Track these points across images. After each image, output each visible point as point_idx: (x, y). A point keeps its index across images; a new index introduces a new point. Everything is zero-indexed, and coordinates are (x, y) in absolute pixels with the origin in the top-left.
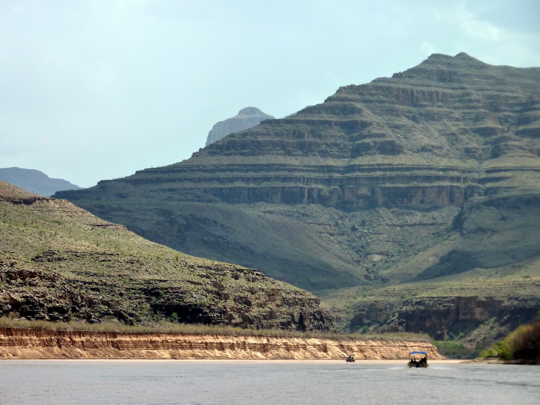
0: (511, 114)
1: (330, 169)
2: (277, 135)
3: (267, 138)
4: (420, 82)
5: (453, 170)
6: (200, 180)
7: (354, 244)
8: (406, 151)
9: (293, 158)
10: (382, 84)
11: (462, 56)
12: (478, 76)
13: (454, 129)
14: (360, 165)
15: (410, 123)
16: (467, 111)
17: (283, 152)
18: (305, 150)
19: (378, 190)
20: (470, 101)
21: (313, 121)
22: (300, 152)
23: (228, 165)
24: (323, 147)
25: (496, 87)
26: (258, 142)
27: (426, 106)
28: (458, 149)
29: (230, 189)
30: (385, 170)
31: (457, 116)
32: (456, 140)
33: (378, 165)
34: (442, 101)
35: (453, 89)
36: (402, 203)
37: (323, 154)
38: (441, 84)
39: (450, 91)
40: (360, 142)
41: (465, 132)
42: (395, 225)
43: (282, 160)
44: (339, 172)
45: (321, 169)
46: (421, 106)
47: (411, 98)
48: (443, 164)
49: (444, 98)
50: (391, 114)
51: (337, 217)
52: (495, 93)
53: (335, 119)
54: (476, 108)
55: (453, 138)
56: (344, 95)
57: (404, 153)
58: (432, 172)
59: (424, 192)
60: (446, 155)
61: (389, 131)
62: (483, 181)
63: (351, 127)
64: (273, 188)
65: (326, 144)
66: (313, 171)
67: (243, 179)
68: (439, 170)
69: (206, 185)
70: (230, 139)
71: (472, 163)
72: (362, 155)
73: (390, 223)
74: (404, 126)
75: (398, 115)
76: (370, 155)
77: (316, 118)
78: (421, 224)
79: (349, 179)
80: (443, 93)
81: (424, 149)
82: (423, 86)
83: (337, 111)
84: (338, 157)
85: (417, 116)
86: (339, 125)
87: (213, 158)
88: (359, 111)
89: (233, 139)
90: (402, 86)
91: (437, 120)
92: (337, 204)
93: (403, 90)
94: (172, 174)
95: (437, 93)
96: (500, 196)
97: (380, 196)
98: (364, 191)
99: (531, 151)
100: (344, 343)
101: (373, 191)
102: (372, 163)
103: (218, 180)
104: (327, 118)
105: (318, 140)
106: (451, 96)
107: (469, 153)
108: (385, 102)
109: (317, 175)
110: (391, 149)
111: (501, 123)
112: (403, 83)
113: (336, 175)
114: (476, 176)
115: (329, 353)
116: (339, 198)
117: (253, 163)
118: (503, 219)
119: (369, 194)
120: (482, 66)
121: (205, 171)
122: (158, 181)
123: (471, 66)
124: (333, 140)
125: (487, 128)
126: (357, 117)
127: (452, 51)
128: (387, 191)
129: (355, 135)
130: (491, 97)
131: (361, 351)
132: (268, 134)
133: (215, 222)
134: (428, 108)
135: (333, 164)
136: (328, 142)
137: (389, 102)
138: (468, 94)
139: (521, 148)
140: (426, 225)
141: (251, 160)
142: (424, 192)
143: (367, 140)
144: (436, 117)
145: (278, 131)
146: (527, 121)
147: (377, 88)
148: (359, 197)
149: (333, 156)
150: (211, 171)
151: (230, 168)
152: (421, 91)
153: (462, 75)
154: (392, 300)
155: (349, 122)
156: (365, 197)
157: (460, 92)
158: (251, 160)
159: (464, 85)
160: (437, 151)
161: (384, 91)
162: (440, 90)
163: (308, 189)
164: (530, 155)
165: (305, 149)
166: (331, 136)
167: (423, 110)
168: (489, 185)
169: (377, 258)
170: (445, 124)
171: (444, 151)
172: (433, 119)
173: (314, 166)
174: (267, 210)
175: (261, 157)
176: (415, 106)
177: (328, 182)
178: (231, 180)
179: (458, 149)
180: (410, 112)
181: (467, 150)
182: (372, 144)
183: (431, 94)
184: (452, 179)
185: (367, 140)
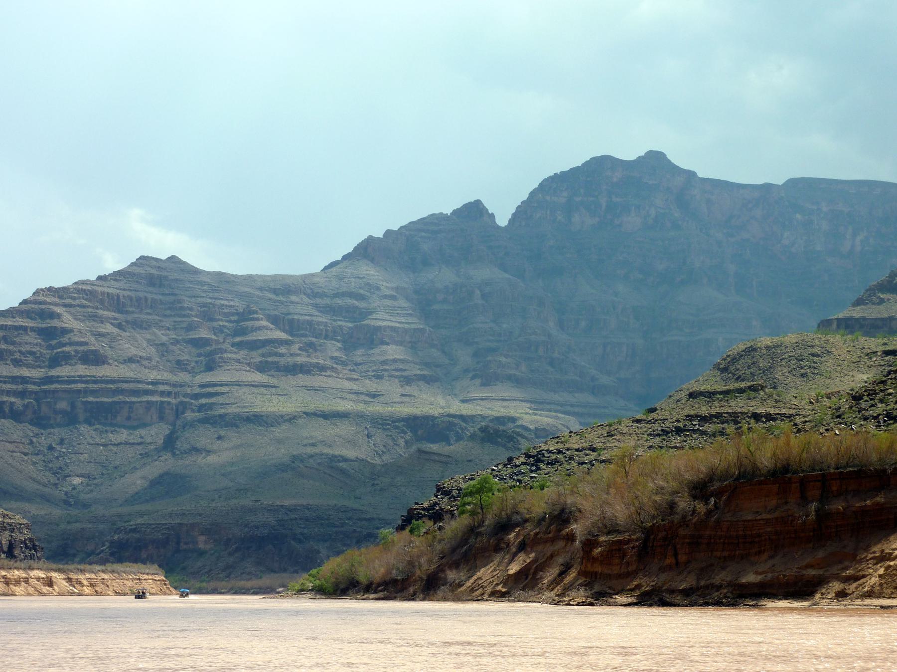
0: (226, 324)
1: (24, 380)
4: (127, 286)
5: (163, 384)
7: (51, 465)
8: (111, 361)
11: (173, 259)
12: (190, 282)
13: (164, 339)
14: (59, 377)
15: (115, 331)
20: (182, 308)
24: (17, 356)
25: (211, 295)
27: (133, 312)
28: (169, 361)
30: (87, 382)
33: (79, 376)
34: (151, 307)
35: (163, 294)
36: (106, 419)
37: (17, 363)
38: (151, 289)
39: (161, 297)
40: (59, 350)
42: (98, 444)
44: (34, 383)
45: (14, 380)
46: (127, 312)
47: (116, 303)
50: (94, 320)
51: (32, 434)
52: (210, 301)
53: (30, 324)
54: (188, 316)
56: (41, 298)
57: (108, 364)
60: (155, 368)
61: (93, 339)
62: (196, 396)
63: (48, 334)
65: (20, 352)
66: (5, 382)
68: (148, 383)
71: (183, 377)
72: (61, 366)
75: (102, 322)
76: (71, 365)
77: (9, 322)
78: (126, 443)
80: (152, 299)
81: (131, 360)
82: (130, 290)
84: (33, 367)
86: (35, 331)
88: (59, 316)
90: (107, 290)
91: (146, 329)
93: (108, 294)
95: (146, 299)
96: (216, 413)
98: (63, 405)
99: (248, 364)
100: (73, 576)
101: (73, 406)
102: (73, 374)
105: (11, 347)
106: (161, 302)
107: (180, 365)
108: (88, 307)
109: (9, 386)
110: (94, 358)
111: (215, 334)
113: (31, 387)
114: (189, 391)
115: (55, 588)
116: (34, 412)
118: (219, 438)
119: (69, 409)
120: (195, 271)
123: (182, 270)
124: (28, 348)
125: (201, 339)
126: (55, 323)
129: (54, 342)
130: (204, 305)
131: (92, 585)
134: (136, 316)
136: (22, 349)
138: (180, 301)
140: (133, 444)
142: (130, 407)
143: (67, 349)
144: (144, 325)
146: (243, 332)
147: (79, 291)
148: (56, 412)
149: (28, 366)
154: (101, 527)
155: (47, 328)
156: (63, 412)
157: (172, 298)
159: (176, 291)
160: (145, 363)
162: (149, 296)
164: (248, 369)
166: (26, 344)
167: (130, 318)
168: (203, 401)
169: (77, 481)
170: (154, 334)
171: (154, 363)
172: (141, 327)
173: (6, 377)
177: (22, 394)
180: (115, 319)
181: (179, 362)
182: (73, 353)
183: (139, 299)
184: (162, 394)
185: (67, 349)
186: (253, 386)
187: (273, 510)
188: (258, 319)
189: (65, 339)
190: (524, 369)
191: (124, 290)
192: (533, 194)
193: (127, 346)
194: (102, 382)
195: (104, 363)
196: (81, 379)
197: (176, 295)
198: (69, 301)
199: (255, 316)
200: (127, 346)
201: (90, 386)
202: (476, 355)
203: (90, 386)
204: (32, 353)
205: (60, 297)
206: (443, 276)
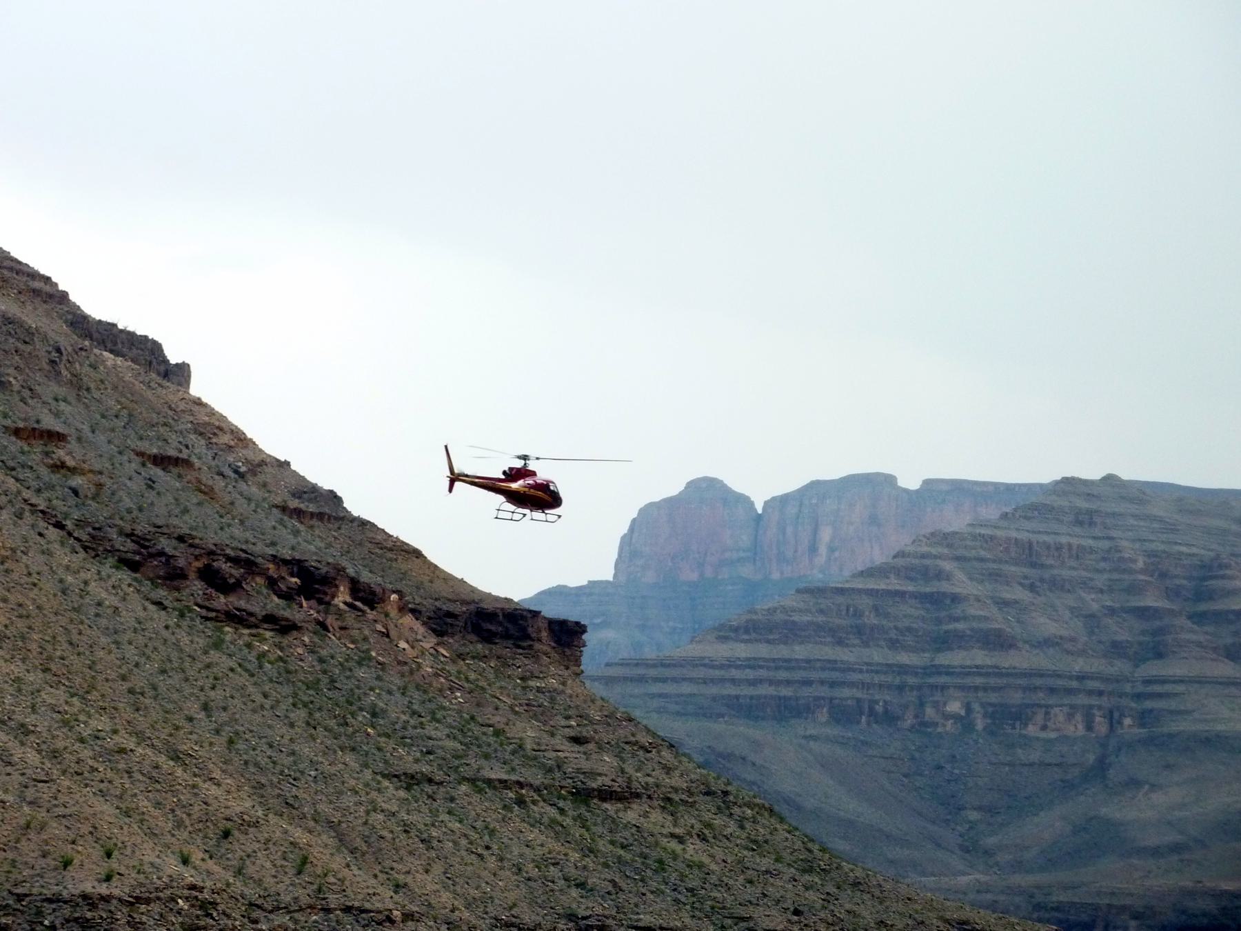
0: (1185, 582)
1: (903, 669)
2: (821, 611)
3: (806, 618)
5: (1092, 678)
6: (705, 682)
8: (1020, 644)
9: (846, 650)
10: (983, 532)
11: (1110, 479)
12: (1135, 516)
13: (1095, 607)
14: (949, 666)
16: (1116, 576)
17: (829, 639)
18: (864, 638)
19: (976, 707)
20: (1121, 559)
21: (877, 591)
22: (857, 642)
23: (748, 659)
25: (1164, 537)
26: (793, 622)
27: (1051, 566)
28: (1100, 642)
29: (751, 698)
30: (987, 675)
31: (1099, 585)
32: (1098, 627)
33: (977, 667)
35: (1094, 538)
36: (1014, 728)
37: (894, 644)
38: (1078, 530)
39: (1091, 542)
40: (951, 627)
41: (1112, 611)
42: (1003, 764)
43: (829, 652)
44: (916, 674)
45: (889, 668)
47: (1029, 554)
48: (1077, 668)
49: (1079, 553)
52: (1162, 547)
55: (1091, 619)
56: (925, 549)
58: (1060, 682)
59: (1047, 713)
60: (1082, 653)
61: (994, 610)
62: (1138, 697)
63: (935, 600)
64: (817, 699)
65: (896, 628)
66: (877, 672)
67: (771, 682)
68: (1071, 678)
69: (714, 690)
70: (748, 617)
71: (1120, 667)
73: (993, 759)
74: (1016, 602)
76: (966, 649)
77: (881, 585)
79: (934, 687)
80: (1079, 546)
81: (1046, 643)
82: (1048, 533)
83: (913, 574)
84: (914, 650)
85: (1038, 584)
87: (725, 646)
89: (755, 617)
90: (1014, 534)
92: (913, 726)
94: (661, 670)
95: (1070, 545)
96: (1165, 730)
97: (979, 716)
98: (955, 707)
99: (1215, 649)
102: (968, 663)
103: (733, 681)
104: (898, 588)
106: (1092, 551)
107: (1117, 649)
109: (883, 678)
111: (1168, 597)
112: (1017, 530)
113: (911, 680)
114: (1128, 688)
116: (916, 716)
117: (787, 657)
118: (1167, 767)
119: (963, 713)
121: (713, 667)
122: (641, 680)
123: (1123, 498)
124: (907, 623)
125: (1147, 609)
126: (945, 587)
127: (1092, 472)
128: (990, 709)
129: (943, 614)
132: (808, 611)
133: (744, 759)
135: (908, 662)
136: (900, 625)
137: (994, 561)
139: (1199, 644)
140: (1049, 765)
141: (782, 651)
142: (1047, 713)
143: (960, 626)
144: (1067, 586)
145: (822, 606)
146: (1211, 596)
147: (974, 537)
148: (947, 717)
149: (907, 649)
150: (722, 667)
151: (752, 663)
152: (1045, 542)
153: (1108, 515)
154: (1017, 899)
156: (956, 717)
157: (1106, 544)
158: (782, 651)
161: (986, 542)
162: (1075, 541)
163: (870, 701)
164: (1214, 656)
165: (864, 635)
166: (905, 616)
167: (1047, 575)
168: (1149, 704)
169: (974, 815)
171: (1080, 646)
172: (1062, 589)
173: (879, 664)
174: (808, 733)
175: (797, 648)
176: (1033, 565)
178: (753, 683)
179: (1100, 642)
180: (1026, 577)
181: (1115, 645)
183: (1059, 548)
184: (1090, 693)
185: (960, 626)
186: (1220, 683)
187: (1218, 895)
188: (1231, 578)
189: (957, 611)
191: (1039, 532)
193: (1042, 620)
194: (1008, 675)
195: (1011, 646)
196: (979, 671)
197: (1111, 538)
198: (961, 552)
199: (1228, 572)
200: (1042, 620)
201: (992, 681)
203: (992, 681)
204: (909, 629)
205: (949, 546)
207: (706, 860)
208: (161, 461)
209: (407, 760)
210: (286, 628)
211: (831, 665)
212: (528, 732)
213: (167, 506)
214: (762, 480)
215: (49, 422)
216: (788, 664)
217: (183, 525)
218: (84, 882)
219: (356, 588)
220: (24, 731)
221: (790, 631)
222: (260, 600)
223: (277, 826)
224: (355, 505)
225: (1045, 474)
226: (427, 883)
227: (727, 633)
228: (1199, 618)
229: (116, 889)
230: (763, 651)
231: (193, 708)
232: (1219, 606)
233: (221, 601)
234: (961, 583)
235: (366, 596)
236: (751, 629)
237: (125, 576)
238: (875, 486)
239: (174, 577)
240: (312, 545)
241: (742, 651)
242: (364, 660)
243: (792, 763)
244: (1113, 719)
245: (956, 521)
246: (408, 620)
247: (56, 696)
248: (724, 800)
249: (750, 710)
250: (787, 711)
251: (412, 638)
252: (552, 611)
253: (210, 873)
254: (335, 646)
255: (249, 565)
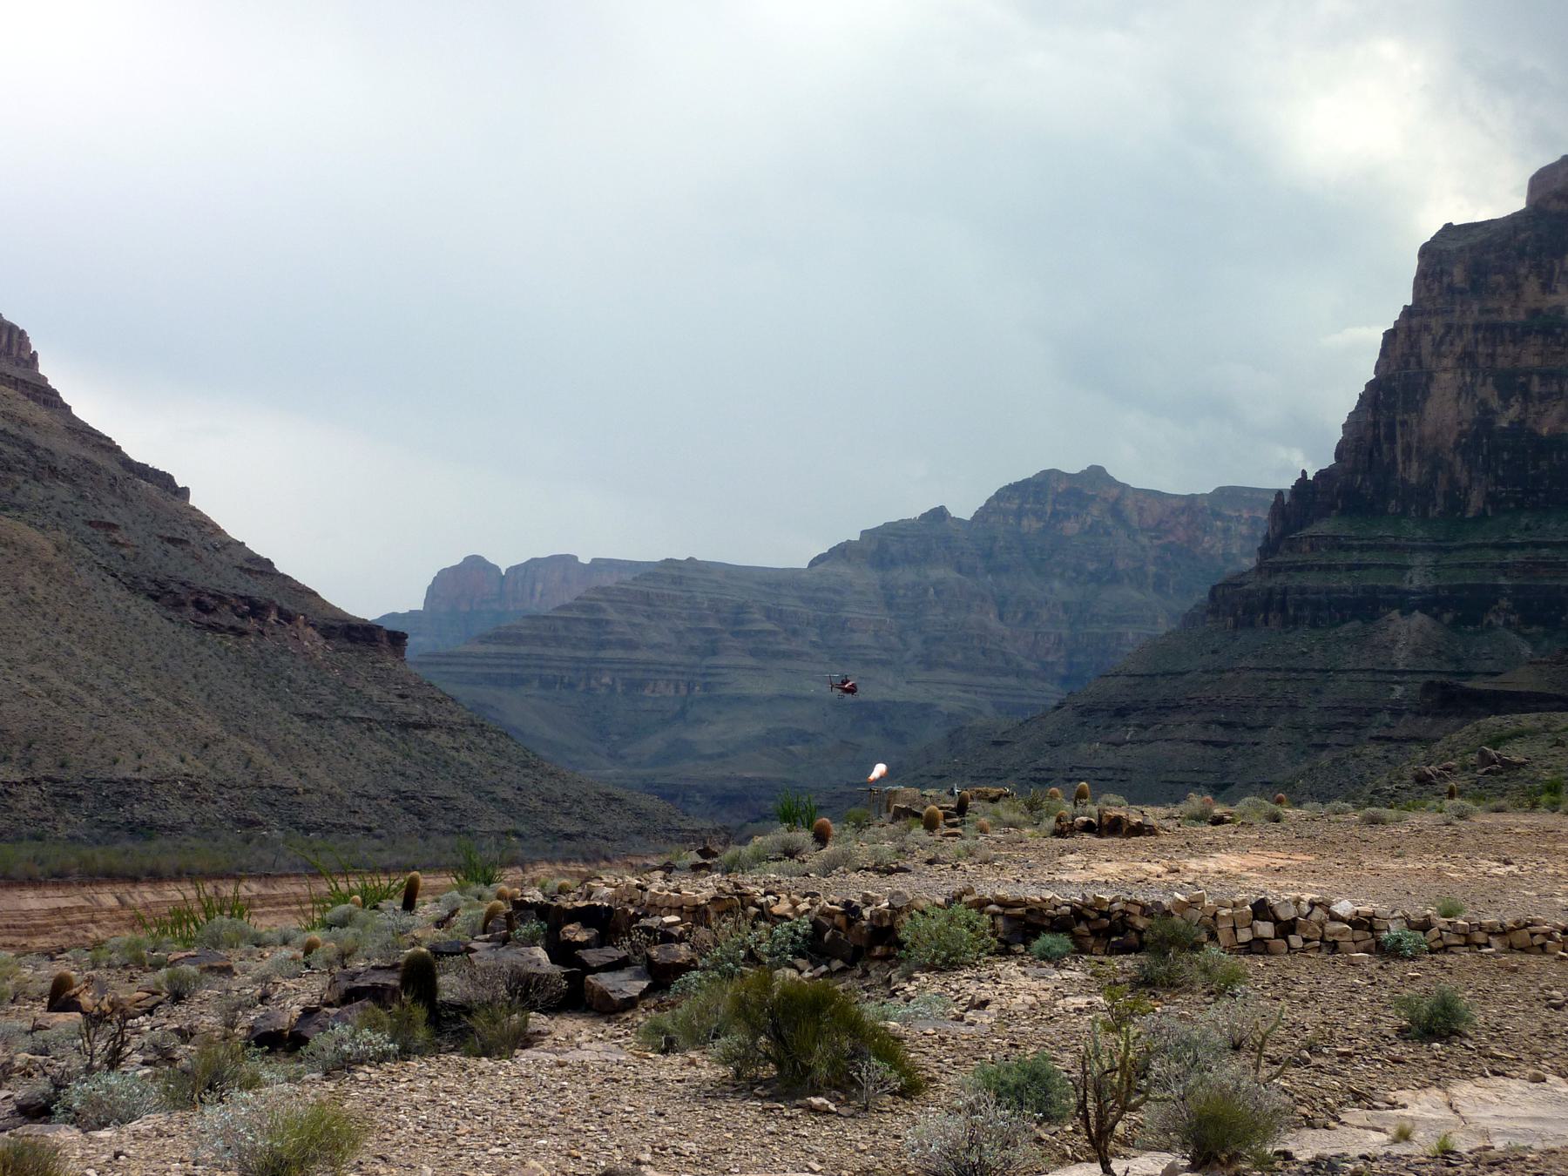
1: (579, 660)
6: (472, 665)
11: (691, 560)
13: (681, 628)
15: (645, 621)
41: (690, 630)
43: (539, 650)
62: (704, 675)
63: (597, 623)
88: (604, 611)
98: (606, 680)
101: (613, 680)
113: (583, 665)
122: (438, 664)
126: (602, 616)
127: (682, 556)
151: (498, 656)
156: (607, 685)
168: (709, 679)
178: (498, 666)
181: (692, 648)
190: (959, 656)
192: (989, 501)
202: (925, 642)
206: (904, 576)
207: (469, 760)
208: (171, 540)
209: (308, 706)
210: (242, 634)
211: (540, 657)
212: (375, 692)
213: (175, 565)
214: (505, 558)
215: (109, 518)
216: (517, 656)
217: (184, 576)
218: (125, 771)
219: (281, 612)
220: (92, 688)
221: (519, 639)
222: (226, 618)
223: (234, 742)
224: (281, 567)
225: (656, 556)
226: (317, 774)
227: (484, 639)
228: (735, 634)
229: (142, 776)
230: (504, 649)
231: (188, 677)
232: (747, 627)
233: (205, 618)
234: (612, 614)
235: (287, 617)
236: (499, 637)
237: (151, 604)
238: (567, 561)
239: (179, 605)
240: (257, 589)
241: (493, 649)
242: (285, 652)
243: (519, 709)
244: (690, 688)
245: (609, 581)
246: (309, 630)
247: (107, 669)
248: (481, 729)
249: (496, 681)
250: (517, 681)
251: (311, 640)
252: (388, 626)
253: (196, 767)
254: (268, 643)
255: (220, 598)
